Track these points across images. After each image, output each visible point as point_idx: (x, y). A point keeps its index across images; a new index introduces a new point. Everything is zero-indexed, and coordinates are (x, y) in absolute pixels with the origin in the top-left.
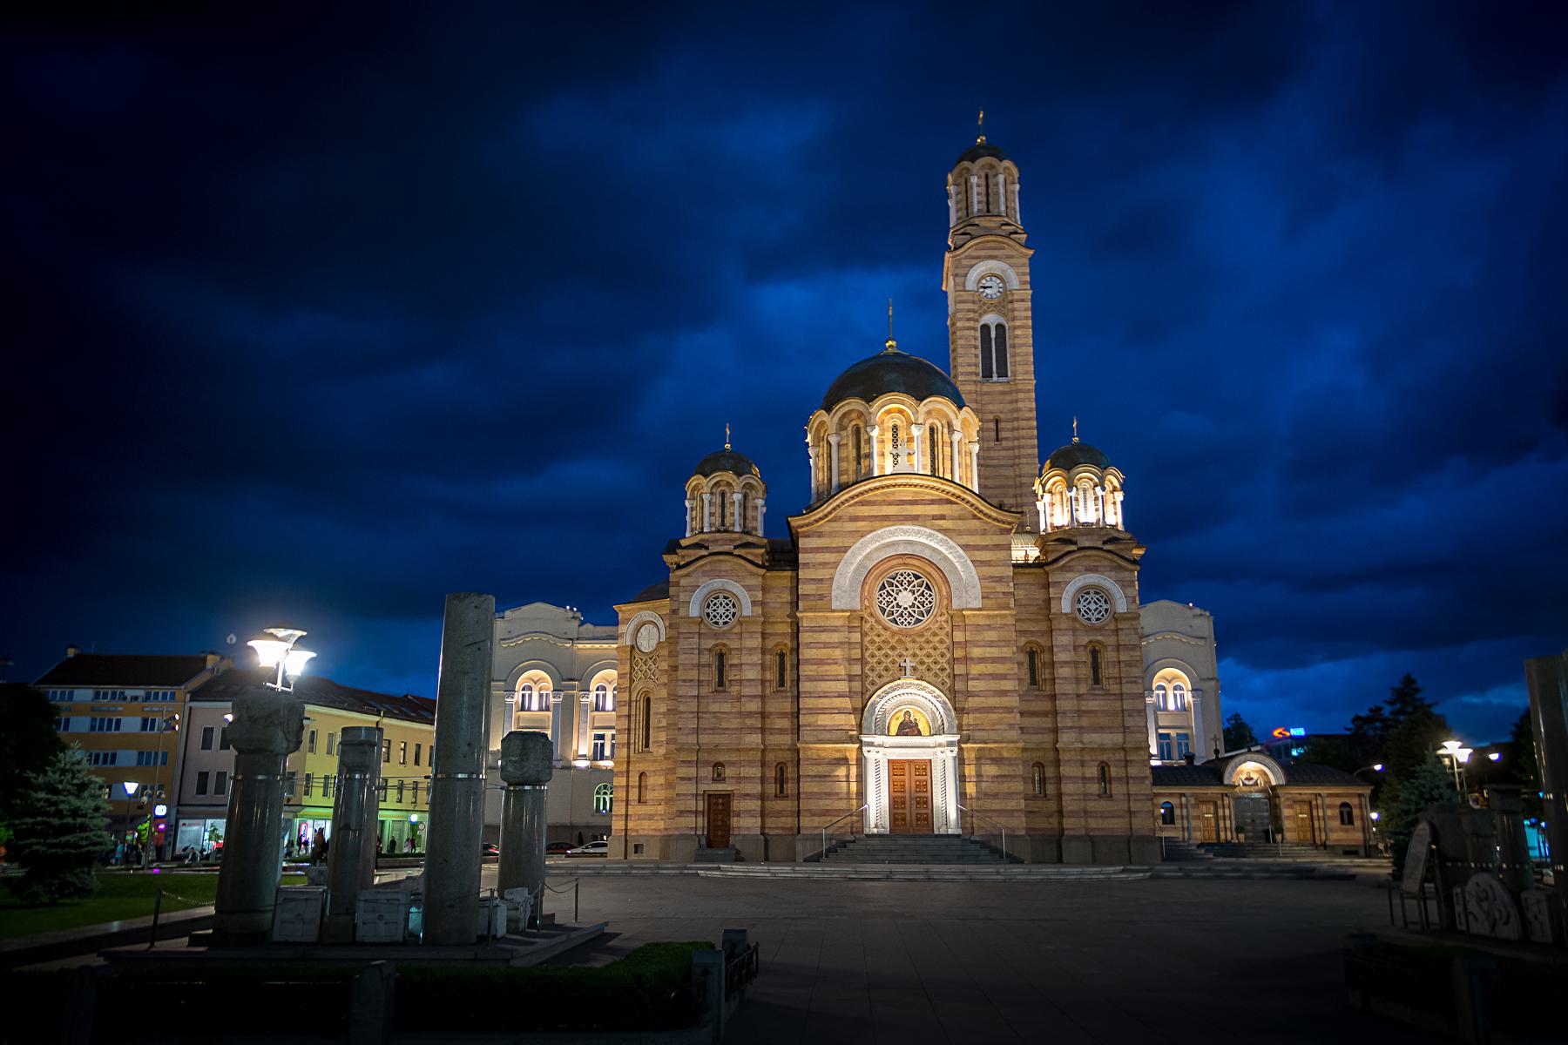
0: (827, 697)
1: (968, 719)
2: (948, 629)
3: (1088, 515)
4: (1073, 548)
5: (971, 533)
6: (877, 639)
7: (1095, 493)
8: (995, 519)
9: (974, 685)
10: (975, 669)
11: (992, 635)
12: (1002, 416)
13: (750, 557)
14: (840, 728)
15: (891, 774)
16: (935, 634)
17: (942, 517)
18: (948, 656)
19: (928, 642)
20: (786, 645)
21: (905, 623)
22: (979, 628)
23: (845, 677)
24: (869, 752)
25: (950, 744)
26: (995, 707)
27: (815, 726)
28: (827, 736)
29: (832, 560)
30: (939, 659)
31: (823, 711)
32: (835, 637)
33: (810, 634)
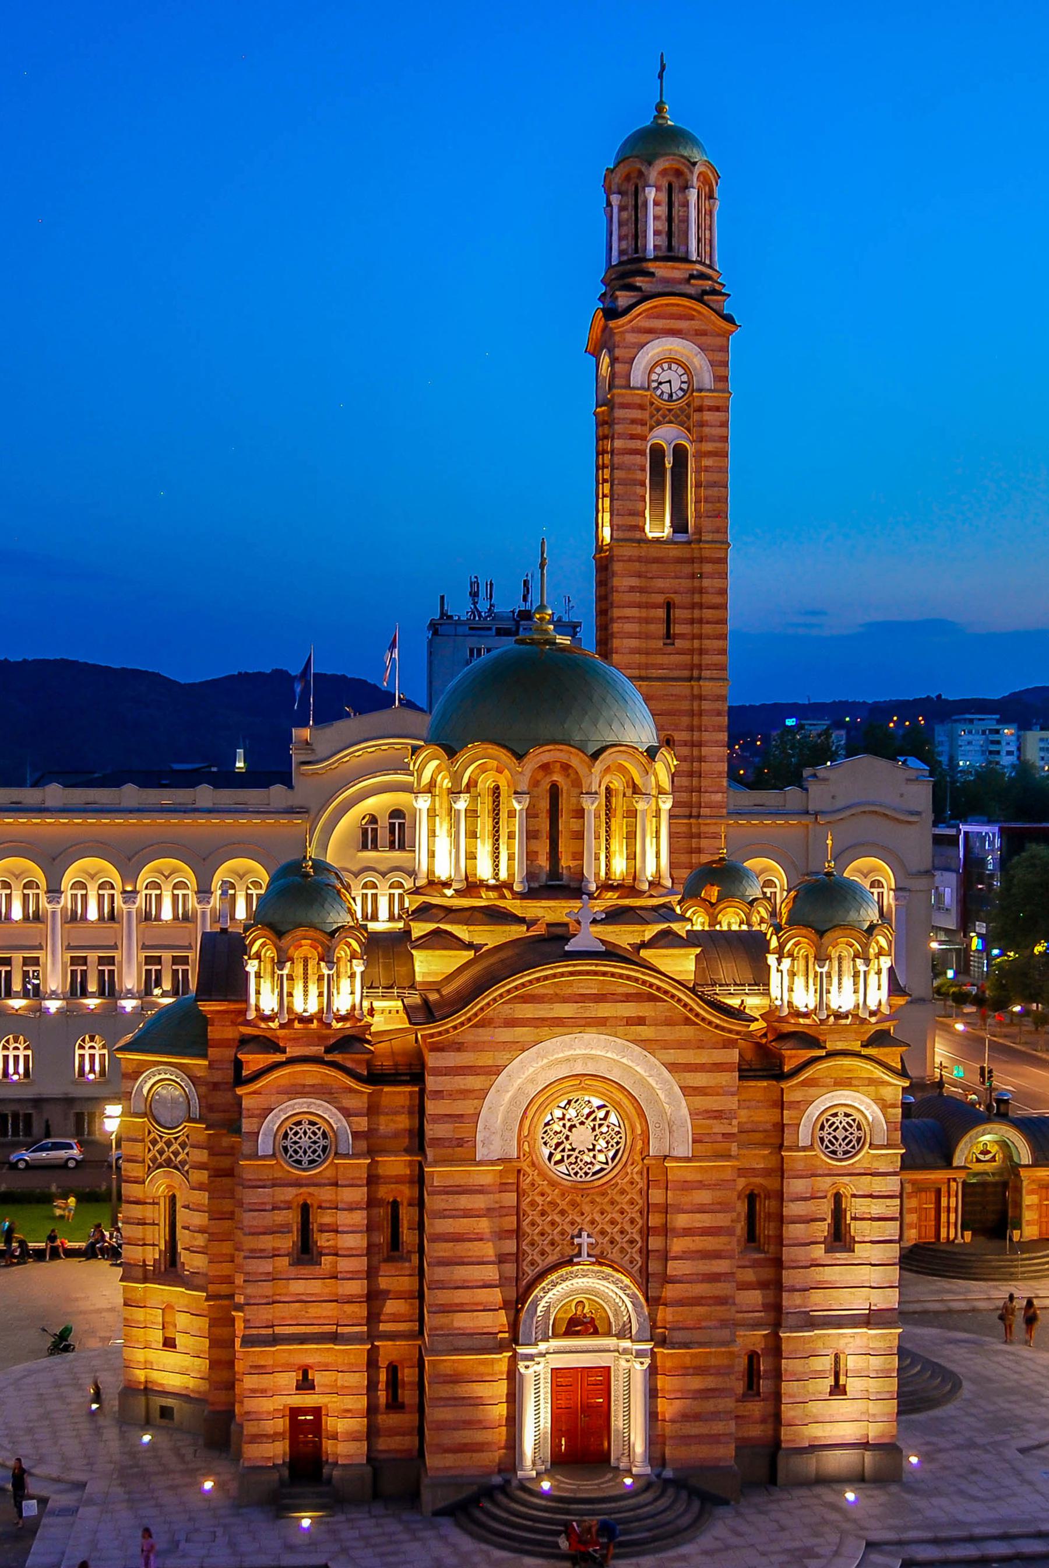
0: (468, 1287)
1: (665, 1314)
2: (642, 1184)
3: (843, 999)
4: (823, 1053)
5: (681, 1045)
6: (539, 1200)
7: (854, 966)
8: (717, 1027)
9: (674, 1268)
10: (677, 1245)
11: (704, 1197)
12: (677, 599)
13: (349, 1065)
14: (485, 1330)
15: (555, 1399)
16: (623, 1192)
17: (641, 1021)
18: (640, 1222)
19: (612, 1203)
20: (401, 1192)
21: (581, 1173)
22: (686, 1186)
23: (493, 1259)
24: (527, 1367)
25: (639, 1354)
26: (702, 1298)
27: (449, 1329)
28: (466, 1343)
29: (478, 1086)
30: (627, 1227)
31: (460, 1308)
32: (479, 1202)
33: (443, 1197)
